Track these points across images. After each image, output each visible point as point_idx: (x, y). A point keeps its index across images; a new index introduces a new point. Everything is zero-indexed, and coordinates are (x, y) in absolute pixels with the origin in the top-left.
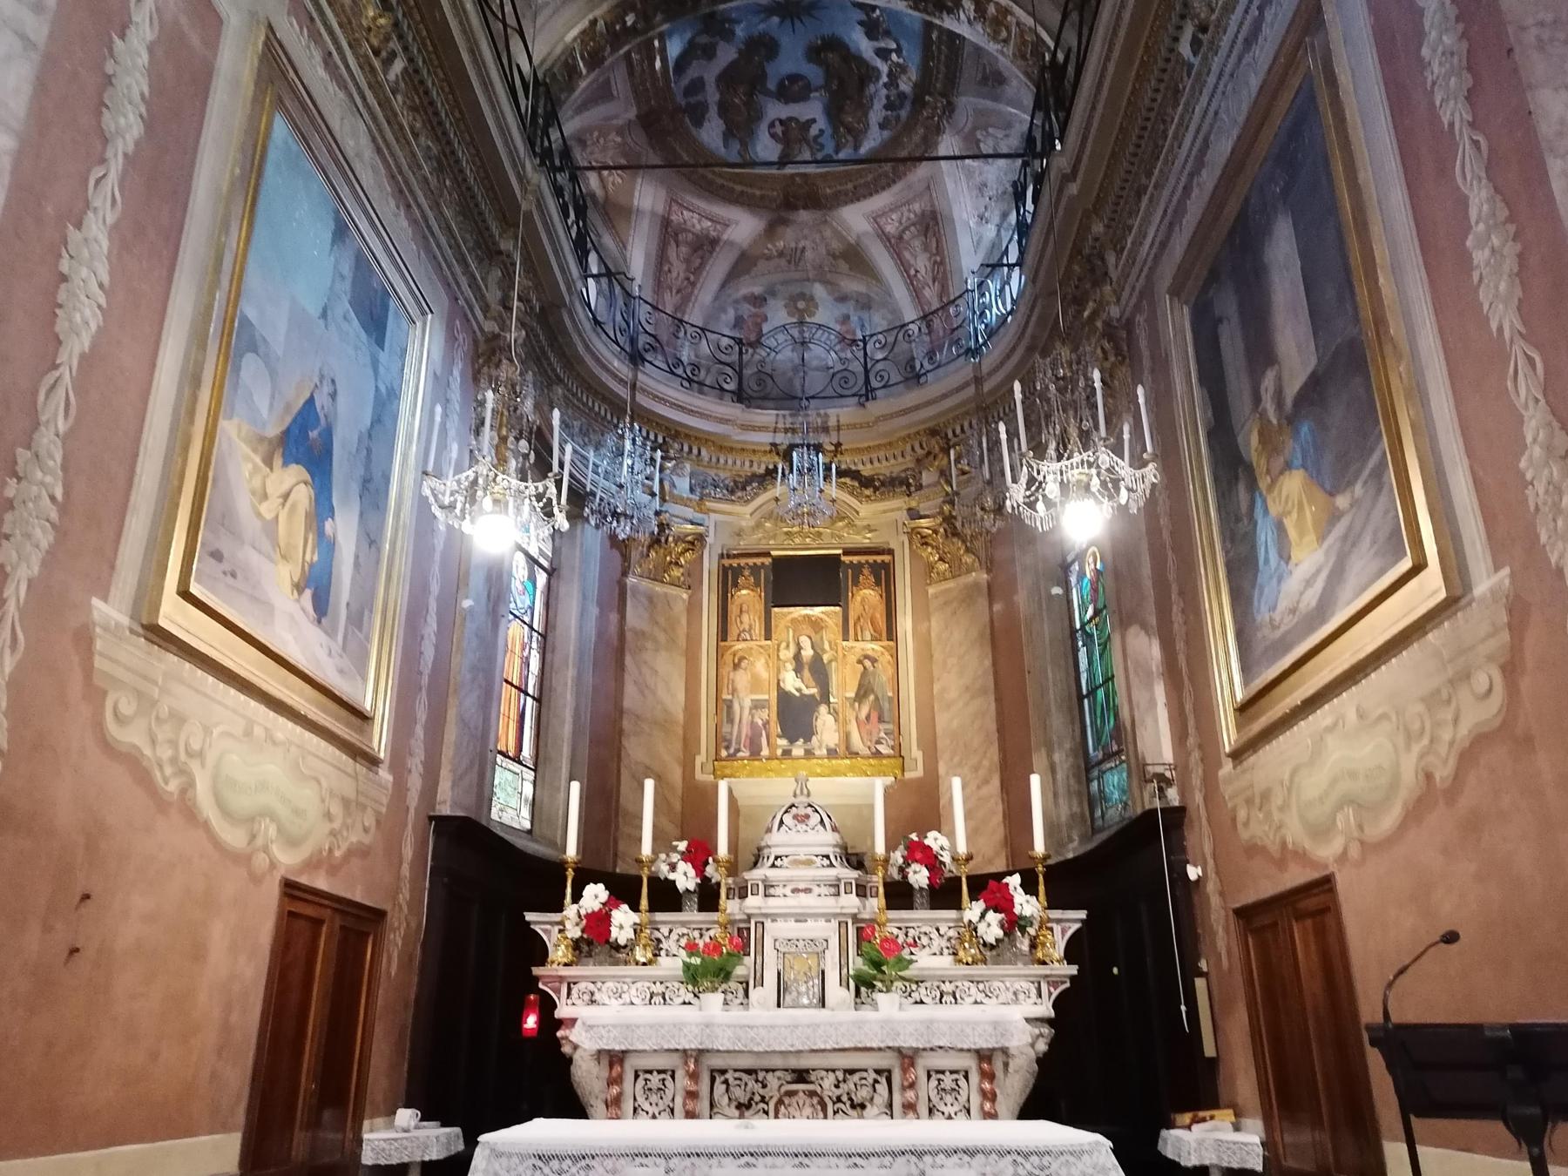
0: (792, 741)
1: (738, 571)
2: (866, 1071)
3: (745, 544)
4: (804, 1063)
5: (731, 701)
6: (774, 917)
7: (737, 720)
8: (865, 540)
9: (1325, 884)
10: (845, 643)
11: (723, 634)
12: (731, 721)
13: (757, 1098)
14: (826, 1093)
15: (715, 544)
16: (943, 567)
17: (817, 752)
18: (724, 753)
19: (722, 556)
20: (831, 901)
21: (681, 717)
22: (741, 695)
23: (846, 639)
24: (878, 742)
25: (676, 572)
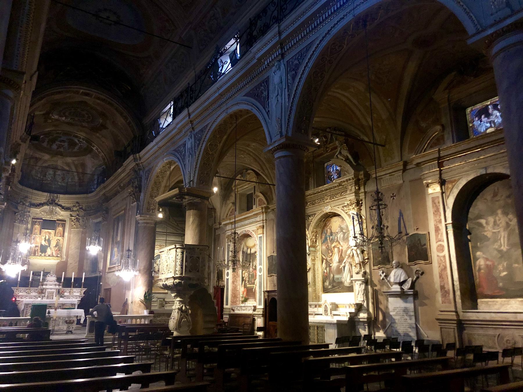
3: (37, 216)
4: (51, 305)
6: (48, 289)
8: (61, 218)
9: (110, 289)
16: (74, 226)
17: (46, 255)
19: (33, 218)
20: (55, 286)
23: (55, 236)
24: (58, 254)
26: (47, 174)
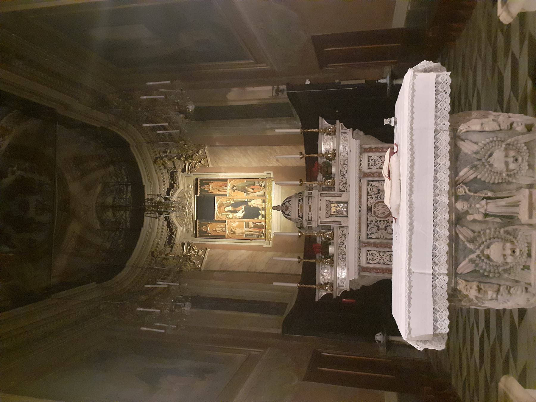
0: (260, 214)
1: (201, 231)
2: (368, 189)
3: (192, 229)
5: (245, 235)
7: (252, 233)
10: (228, 196)
11: (223, 237)
12: (252, 235)
13: (376, 224)
14: (375, 202)
15: (191, 239)
16: (203, 162)
18: (263, 237)
21: (250, 252)
22: (244, 231)
24: (261, 186)
25: (200, 253)
26: (114, 220)
